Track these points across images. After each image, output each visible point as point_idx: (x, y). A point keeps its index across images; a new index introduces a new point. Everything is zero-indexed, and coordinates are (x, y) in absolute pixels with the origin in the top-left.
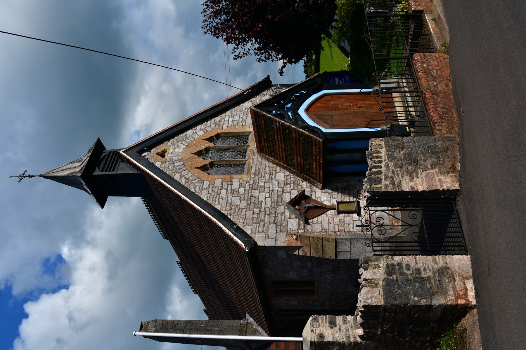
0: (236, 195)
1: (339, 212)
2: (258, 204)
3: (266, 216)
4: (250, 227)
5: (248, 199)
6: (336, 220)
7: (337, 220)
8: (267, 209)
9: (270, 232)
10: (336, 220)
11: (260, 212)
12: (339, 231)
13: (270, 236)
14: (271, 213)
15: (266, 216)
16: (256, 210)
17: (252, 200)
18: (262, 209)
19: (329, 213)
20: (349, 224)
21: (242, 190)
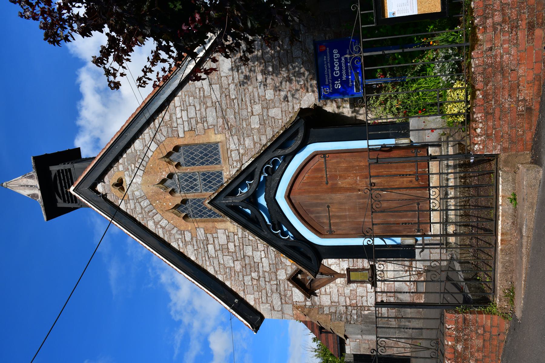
0: (227, 254)
1: (349, 282)
2: (255, 267)
3: (267, 283)
4: (252, 296)
5: (241, 258)
6: (347, 291)
7: (349, 291)
8: (266, 274)
9: (274, 303)
10: (347, 291)
11: (259, 277)
12: (350, 306)
13: (276, 308)
14: (271, 280)
15: (267, 283)
16: (254, 275)
17: (247, 262)
18: (261, 274)
19: (338, 280)
20: (362, 297)
21: (231, 246)
